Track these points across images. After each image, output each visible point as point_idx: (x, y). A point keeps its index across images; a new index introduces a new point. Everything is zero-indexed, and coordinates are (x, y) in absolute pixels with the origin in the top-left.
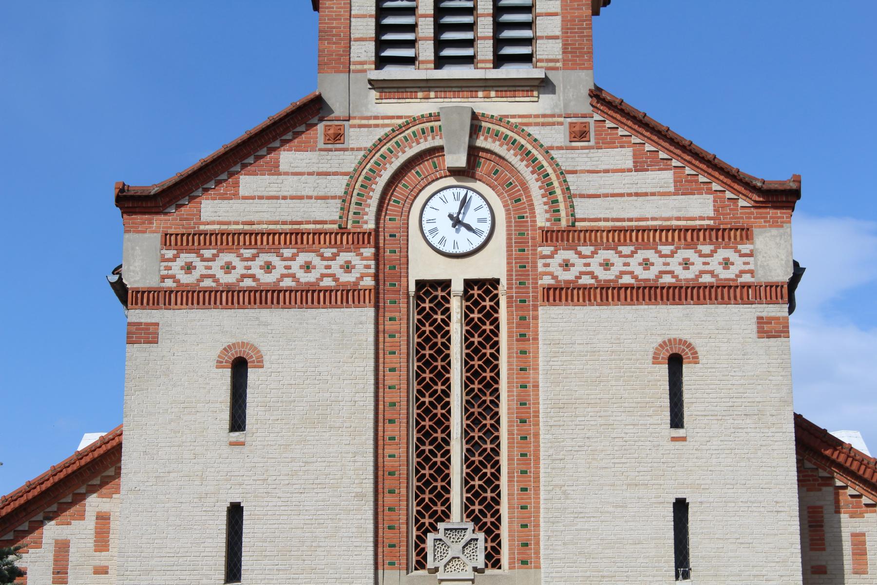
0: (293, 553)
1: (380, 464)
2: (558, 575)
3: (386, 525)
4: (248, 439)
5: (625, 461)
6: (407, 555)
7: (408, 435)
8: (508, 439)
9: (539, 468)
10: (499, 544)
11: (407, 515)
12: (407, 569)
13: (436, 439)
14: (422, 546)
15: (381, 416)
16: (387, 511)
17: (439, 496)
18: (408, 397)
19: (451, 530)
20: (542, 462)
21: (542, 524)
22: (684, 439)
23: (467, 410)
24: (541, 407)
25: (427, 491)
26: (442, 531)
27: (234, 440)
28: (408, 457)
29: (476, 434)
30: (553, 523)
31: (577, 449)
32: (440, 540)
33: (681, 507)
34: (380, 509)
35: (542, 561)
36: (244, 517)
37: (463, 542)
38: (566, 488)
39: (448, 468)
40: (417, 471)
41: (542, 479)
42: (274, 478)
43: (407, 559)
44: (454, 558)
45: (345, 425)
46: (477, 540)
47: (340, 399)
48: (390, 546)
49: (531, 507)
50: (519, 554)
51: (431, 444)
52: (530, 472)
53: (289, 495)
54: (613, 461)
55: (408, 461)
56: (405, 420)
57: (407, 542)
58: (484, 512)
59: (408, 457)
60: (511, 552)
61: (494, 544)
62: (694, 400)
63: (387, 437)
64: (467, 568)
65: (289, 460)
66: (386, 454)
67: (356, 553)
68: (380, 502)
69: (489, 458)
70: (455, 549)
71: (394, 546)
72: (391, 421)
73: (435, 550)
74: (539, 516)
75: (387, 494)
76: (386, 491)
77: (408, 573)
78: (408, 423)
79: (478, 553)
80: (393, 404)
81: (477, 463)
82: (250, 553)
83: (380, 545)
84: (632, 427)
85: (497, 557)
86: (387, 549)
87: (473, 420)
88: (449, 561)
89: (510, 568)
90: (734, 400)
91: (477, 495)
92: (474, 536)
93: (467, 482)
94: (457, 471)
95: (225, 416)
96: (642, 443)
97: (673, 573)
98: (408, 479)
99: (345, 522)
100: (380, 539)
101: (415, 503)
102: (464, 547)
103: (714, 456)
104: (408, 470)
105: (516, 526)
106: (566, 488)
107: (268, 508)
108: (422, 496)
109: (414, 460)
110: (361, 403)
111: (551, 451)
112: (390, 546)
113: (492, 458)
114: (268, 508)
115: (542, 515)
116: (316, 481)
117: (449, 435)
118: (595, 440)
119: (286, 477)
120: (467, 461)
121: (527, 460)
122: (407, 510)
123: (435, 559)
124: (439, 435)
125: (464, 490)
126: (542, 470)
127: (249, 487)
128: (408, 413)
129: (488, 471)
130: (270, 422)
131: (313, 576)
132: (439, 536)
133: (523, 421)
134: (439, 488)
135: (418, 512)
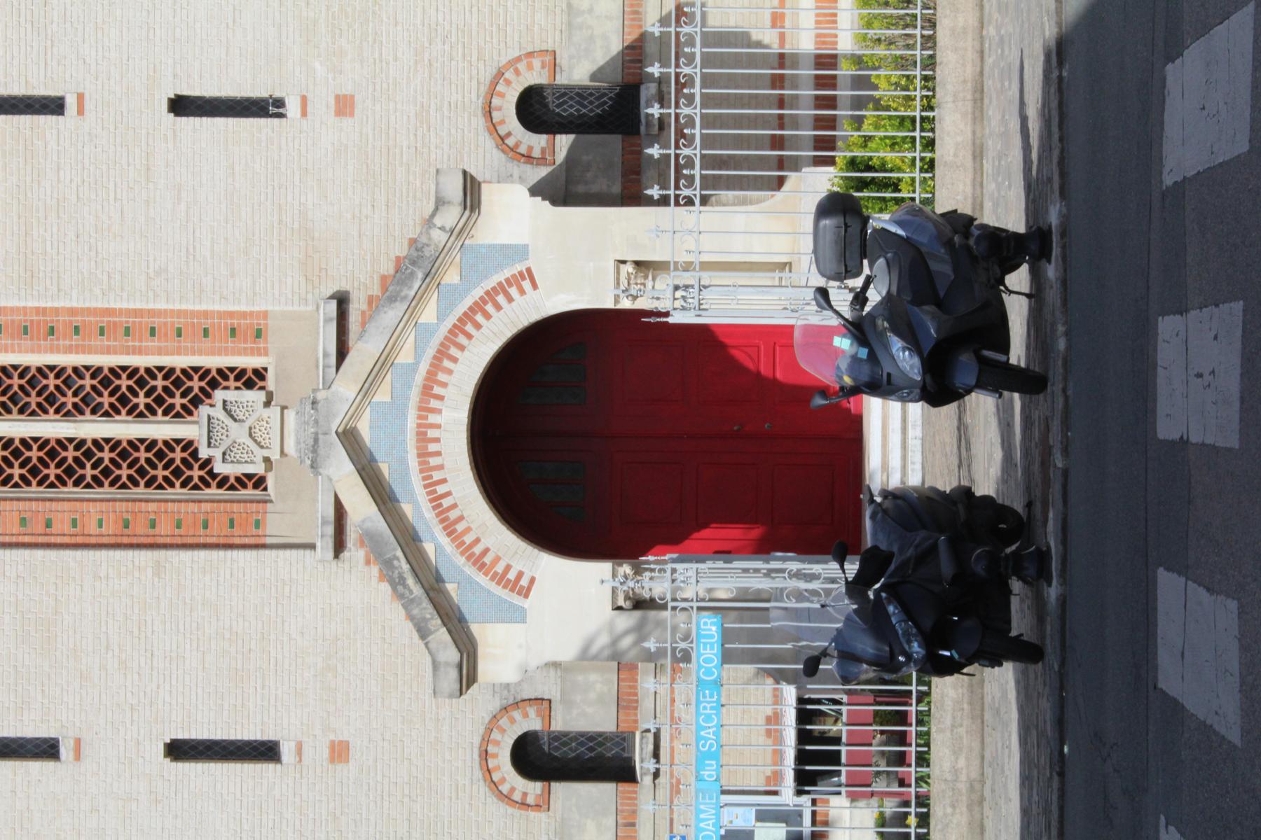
0: (239, 667)
1: (112, 540)
3: (202, 532)
5: (112, 183)
6: (245, 501)
7: (69, 500)
8: (77, 353)
9: (121, 310)
10: (232, 369)
11: (187, 501)
12: (266, 502)
13: (76, 459)
14: (232, 480)
15: (41, 540)
16: (181, 531)
17: (160, 455)
18: (12, 499)
19: (209, 438)
20: (113, 305)
21: (204, 307)
22: (81, 97)
23: (33, 413)
24: (30, 304)
25: (153, 472)
28: (102, 500)
29: (70, 400)
30: (202, 291)
31: (93, 254)
32: (224, 454)
33: (181, 106)
34: (179, 541)
35: (256, 309)
36: (186, 737)
37: (228, 421)
38: (151, 271)
39: (119, 443)
40: (124, 486)
41: (138, 306)
42: (129, 694)
43: (252, 501)
44: (250, 435)
45: (52, 591)
46: (225, 402)
47: (13, 599)
48: (232, 526)
49: (179, 322)
50: (245, 341)
51: (83, 466)
53: (155, 673)
54: (112, 202)
56: (48, 503)
57: (226, 501)
58: (185, 390)
59: (102, 500)
60: (244, 352)
61: (232, 377)
62: (23, 78)
63: (73, 531)
64: (265, 416)
66: (98, 531)
67: (241, 575)
68: (168, 540)
69: (106, 382)
70: (238, 433)
71: (232, 521)
72: (48, 524)
73: (238, 462)
74: (192, 312)
75: (156, 531)
76: (151, 531)
77: (271, 501)
78: (51, 500)
79: (244, 400)
80: (23, 522)
81: (113, 400)
82: (239, 727)
83: (230, 541)
84: (62, 173)
85: (250, 374)
86: (236, 531)
87: (50, 404)
88: (255, 441)
89: (266, 354)
90: (23, 19)
91: (159, 401)
92: (220, 405)
93: (141, 415)
94: (123, 429)
95: (36, 768)
97: (276, 121)
98: (134, 500)
100: (222, 541)
101: (170, 490)
102: (235, 420)
103: (107, 54)
104: (121, 500)
105: (207, 344)
106: (151, 271)
108: (160, 480)
109: (107, 491)
110: (21, 567)
111: (98, 292)
112: (232, 526)
113: (105, 378)
114: (174, 702)
115: (191, 307)
117: (71, 440)
118: (80, 226)
121: (109, 326)
122: (180, 501)
123: (252, 462)
124: (70, 454)
125: (152, 418)
126: (125, 305)
127: (142, 731)
128: (37, 500)
129: (124, 383)
130: (46, 701)
131: (273, 637)
133: (52, 331)
134: (150, 455)
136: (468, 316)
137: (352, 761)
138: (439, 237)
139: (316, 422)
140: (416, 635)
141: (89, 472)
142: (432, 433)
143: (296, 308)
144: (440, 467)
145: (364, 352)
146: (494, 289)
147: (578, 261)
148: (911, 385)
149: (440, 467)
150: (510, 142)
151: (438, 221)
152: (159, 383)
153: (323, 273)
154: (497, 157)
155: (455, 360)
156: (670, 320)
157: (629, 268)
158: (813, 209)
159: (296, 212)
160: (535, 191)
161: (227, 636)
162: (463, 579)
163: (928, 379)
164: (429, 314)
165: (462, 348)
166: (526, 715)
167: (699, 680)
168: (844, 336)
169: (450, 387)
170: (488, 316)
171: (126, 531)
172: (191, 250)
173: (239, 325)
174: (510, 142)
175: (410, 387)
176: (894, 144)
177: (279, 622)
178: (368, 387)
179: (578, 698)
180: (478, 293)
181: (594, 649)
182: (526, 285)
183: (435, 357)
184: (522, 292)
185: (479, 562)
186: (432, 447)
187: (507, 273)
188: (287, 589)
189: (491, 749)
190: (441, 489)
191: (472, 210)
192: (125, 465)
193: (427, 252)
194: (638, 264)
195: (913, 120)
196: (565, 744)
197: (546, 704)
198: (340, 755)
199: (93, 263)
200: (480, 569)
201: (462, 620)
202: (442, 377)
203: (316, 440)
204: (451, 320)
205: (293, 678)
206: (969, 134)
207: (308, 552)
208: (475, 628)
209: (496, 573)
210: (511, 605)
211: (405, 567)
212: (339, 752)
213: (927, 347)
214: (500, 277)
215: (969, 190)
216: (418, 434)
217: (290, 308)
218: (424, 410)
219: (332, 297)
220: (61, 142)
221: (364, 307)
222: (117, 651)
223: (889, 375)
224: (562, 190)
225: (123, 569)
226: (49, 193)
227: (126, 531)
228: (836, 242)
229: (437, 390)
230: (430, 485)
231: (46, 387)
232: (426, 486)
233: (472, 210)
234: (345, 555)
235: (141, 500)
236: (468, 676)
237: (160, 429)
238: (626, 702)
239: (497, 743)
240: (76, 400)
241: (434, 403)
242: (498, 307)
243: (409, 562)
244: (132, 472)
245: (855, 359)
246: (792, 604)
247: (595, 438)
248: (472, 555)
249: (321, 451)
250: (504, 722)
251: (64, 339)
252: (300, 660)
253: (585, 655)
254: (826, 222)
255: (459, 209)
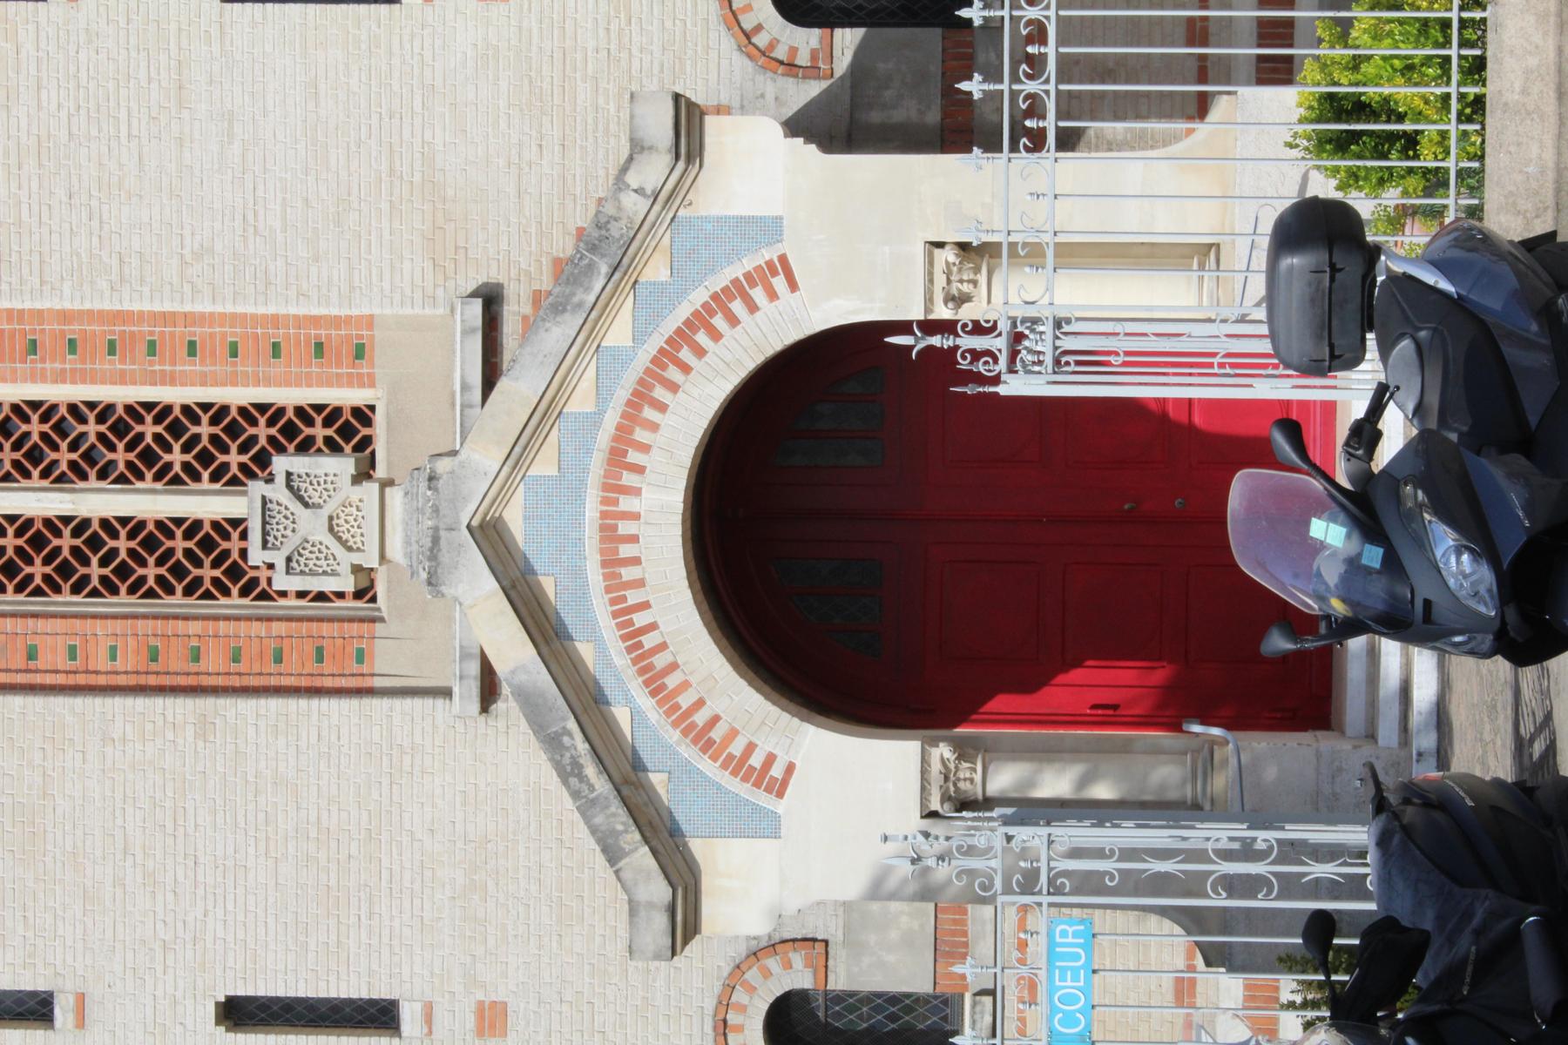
0: (333, 882)
2: (387, 276)
3: (273, 668)
4: (69, 986)
6: (341, 620)
7: (64, 616)
8: (74, 382)
9: (141, 314)
10: (319, 408)
11: (249, 619)
12: (373, 620)
13: (75, 551)
15: (20, 679)
19: (265, 533)
20: (126, 307)
25: (196, 572)
26: (269, 556)
27: (71, 1018)
28: (114, 617)
29: (64, 457)
30: (268, 284)
31: (95, 223)
32: (289, 559)
34: (236, 682)
35: (355, 312)
36: (251, 993)
37: (295, 506)
38: (187, 251)
39: (141, 524)
40: (151, 594)
41: (168, 307)
42: (160, 925)
43: (351, 620)
44: (331, 529)
46: (289, 474)
48: (320, 659)
49: (233, 333)
50: (339, 365)
51: (86, 562)
52: (152, 333)
53: (200, 892)
54: (124, 141)
55: (125, 617)
56: (30, 621)
57: (310, 619)
58: (237, 442)
59: (114, 617)
60: (338, 381)
61: (319, 420)
63: (70, 665)
65: (119, 891)
66: (109, 666)
67: (334, 738)
68: (220, 681)
69: (120, 429)
70: (311, 525)
72: (32, 654)
73: (313, 573)
74: (254, 317)
75: (202, 666)
76: (193, 667)
77: (382, 620)
78: (35, 615)
79: (321, 472)
81: (131, 456)
82: (333, 979)
83: (318, 682)
85: (347, 415)
86: (327, 667)
88: (339, 539)
89: (372, 385)
91: (205, 458)
92: (280, 479)
94: (149, 503)
96: (83, 70)
98: (166, 617)
99: (263, 764)
100: (304, 682)
101: (223, 601)
102: (306, 505)
104: (145, 617)
105: (278, 368)
106: (187, 251)
107: (230, 938)
108: (207, 584)
109: (124, 601)
111: (103, 284)
112: (320, 659)
113: (120, 422)
114: (230, 938)
115: (250, 309)
116: (170, 830)
117: (66, 520)
118: (75, 179)
119: (160, 897)
120: (127, 478)
121: (123, 340)
122: (237, 618)
123: (334, 573)
124: (66, 542)
125: (194, 486)
126: (147, 307)
128: (14, 615)
129: (149, 429)
130: (30, 934)
132: (280, 564)
133: (33, 347)
134: (190, 544)
135: (244, 592)
136: (683, 336)
137: (512, 1035)
138: (634, 205)
139: (436, 510)
140: (600, 860)
141: (95, 571)
142: (625, 528)
143: (418, 311)
144: (640, 583)
145: (521, 387)
146: (725, 290)
147: (859, 241)
148: (1472, 625)
149: (640, 583)
150: (761, 40)
151: (633, 179)
152: (205, 430)
153: (460, 257)
154: (741, 64)
155: (662, 408)
156: (1002, 390)
157: (949, 255)
158: (1267, 226)
159: (417, 156)
160: (796, 126)
161: (313, 834)
162: (678, 773)
163: (1512, 615)
164: (619, 333)
165: (673, 387)
166: (788, 965)
167: (1051, 1032)
168: (1332, 519)
169: (654, 451)
170: (716, 336)
171: (154, 667)
172: (250, 218)
173: (329, 337)
174: (761, 40)
175: (589, 452)
176: (1409, 69)
177: (387, 820)
178: (519, 454)
179: (872, 938)
180: (699, 297)
181: (892, 883)
182: (779, 283)
183: (629, 403)
184: (772, 295)
185: (702, 739)
186: (626, 551)
187: (748, 264)
188: (407, 760)
189: (733, 1018)
190: (640, 620)
191: (689, 160)
192: (151, 561)
193: (615, 230)
194: (963, 247)
195: (1445, 24)
196: (851, 1009)
197: (820, 947)
198: (492, 1026)
199: (95, 240)
200: (704, 750)
201: (675, 832)
202: (640, 435)
203: (436, 540)
204: (656, 342)
205: (417, 902)
206: (1552, 55)
207: (440, 702)
208: (696, 846)
209: (731, 757)
210: (757, 809)
211: (582, 747)
212: (491, 1018)
213: (1510, 549)
214: (737, 271)
215: (1549, 156)
216: (603, 528)
217: (408, 311)
218: (613, 489)
219: (474, 295)
220: (43, 45)
221: (527, 309)
222: (139, 860)
223: (1427, 604)
224: (838, 125)
225: (149, 726)
226: (24, 124)
227: (154, 667)
228: (1313, 301)
229: (633, 457)
230: (623, 613)
231: (27, 435)
232: (615, 615)
233: (689, 160)
234: (499, 706)
235: (176, 617)
236: (685, 924)
237: (205, 504)
238: (948, 945)
239: (742, 1009)
240: (74, 456)
241: (628, 479)
242: (733, 321)
243: (587, 738)
244: (162, 571)
245: (1353, 565)
246: (1220, 901)
247: (889, 537)
248: (693, 725)
249: (445, 557)
250: (753, 975)
251: (53, 361)
252: (428, 873)
253: (876, 891)
254: (1293, 262)
255: (666, 159)
